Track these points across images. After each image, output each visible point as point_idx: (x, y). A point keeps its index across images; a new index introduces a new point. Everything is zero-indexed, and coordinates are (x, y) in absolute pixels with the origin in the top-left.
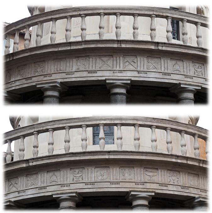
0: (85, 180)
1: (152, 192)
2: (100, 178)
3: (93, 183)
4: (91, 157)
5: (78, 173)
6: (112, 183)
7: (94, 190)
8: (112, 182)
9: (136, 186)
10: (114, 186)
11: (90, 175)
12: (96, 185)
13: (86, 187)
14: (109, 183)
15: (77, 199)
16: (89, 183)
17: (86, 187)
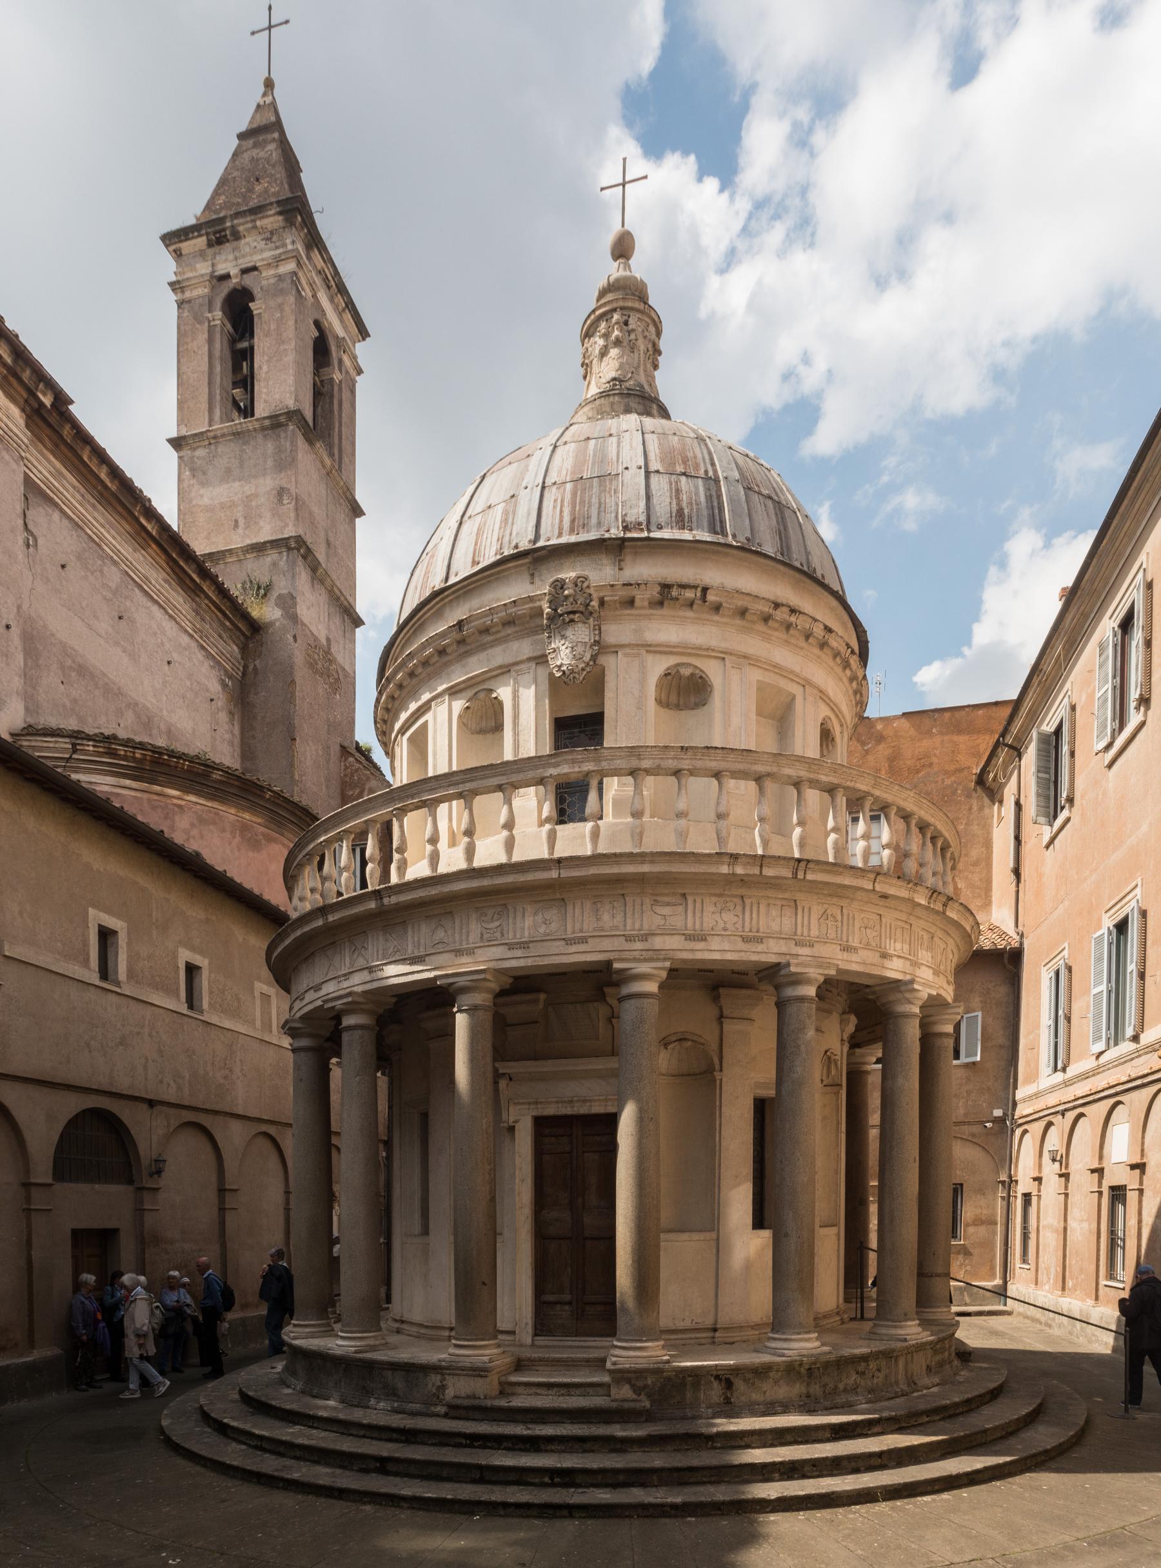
0: (510, 938)
1: (665, 960)
2: (542, 930)
3: (524, 945)
4: (516, 876)
5: (492, 920)
6: (569, 942)
7: (529, 962)
8: (570, 939)
9: (627, 946)
10: (574, 949)
11: (518, 924)
12: (535, 950)
13: (510, 954)
14: (563, 943)
15: (492, 985)
16: (517, 943)
17: (510, 954)
